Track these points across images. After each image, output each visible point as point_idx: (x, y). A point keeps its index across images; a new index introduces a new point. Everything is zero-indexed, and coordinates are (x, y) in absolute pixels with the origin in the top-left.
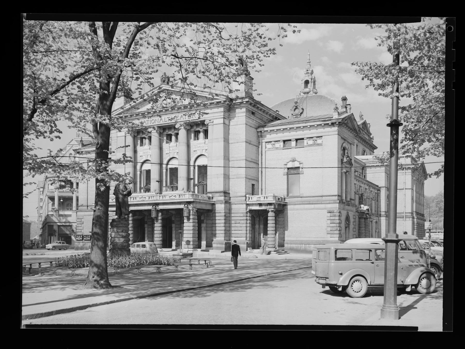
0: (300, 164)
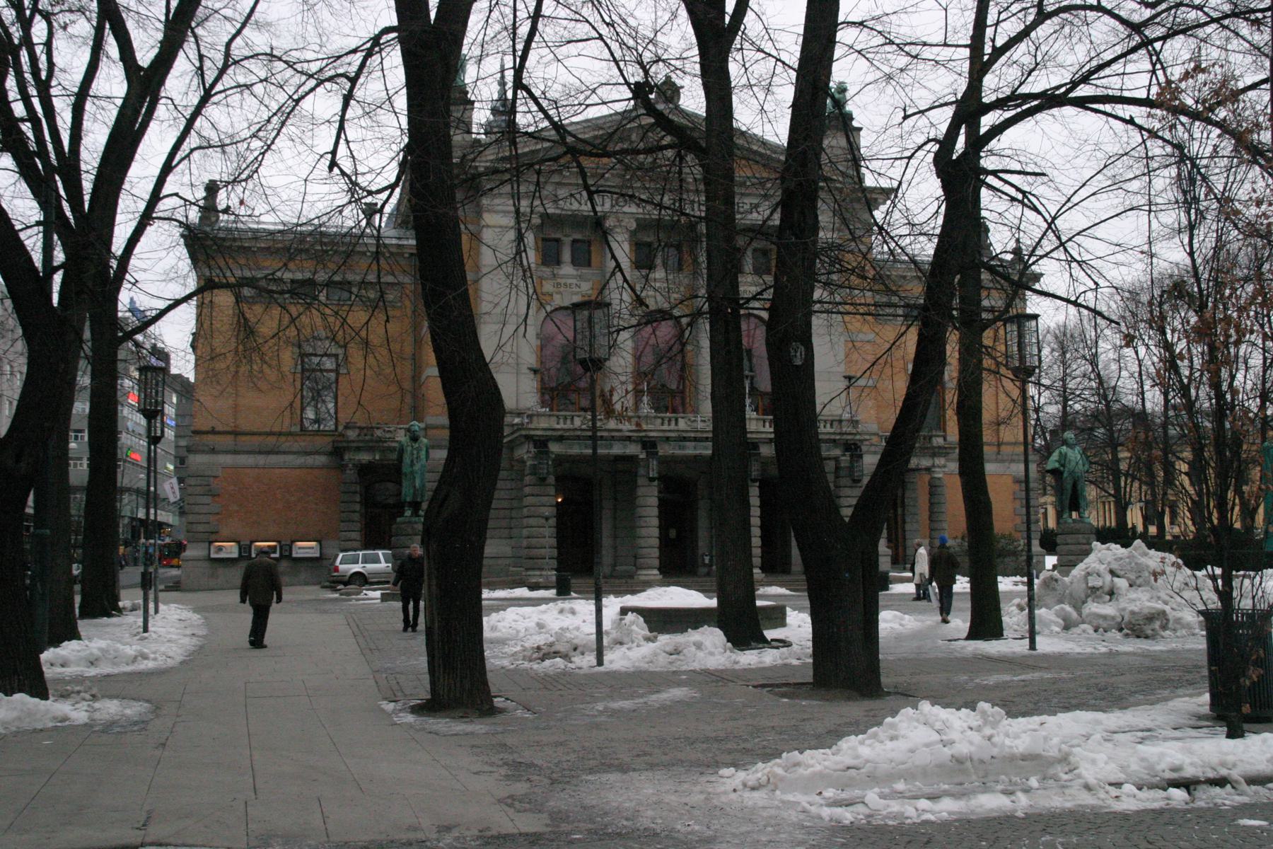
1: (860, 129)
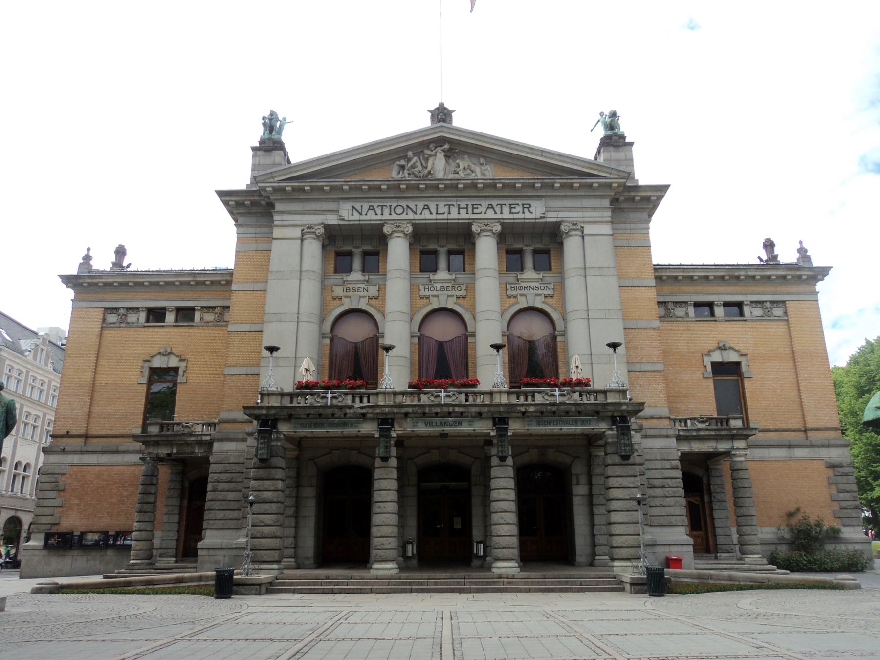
0: (742, 355)
1: (631, 144)
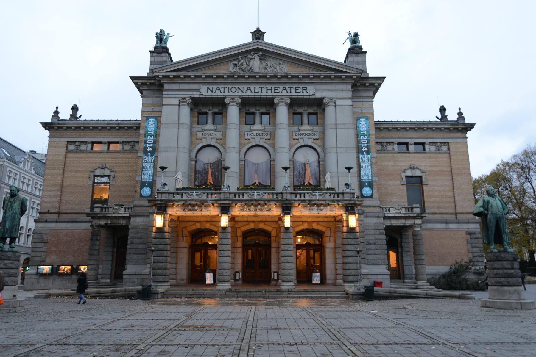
0: (423, 172)
1: (365, 52)
